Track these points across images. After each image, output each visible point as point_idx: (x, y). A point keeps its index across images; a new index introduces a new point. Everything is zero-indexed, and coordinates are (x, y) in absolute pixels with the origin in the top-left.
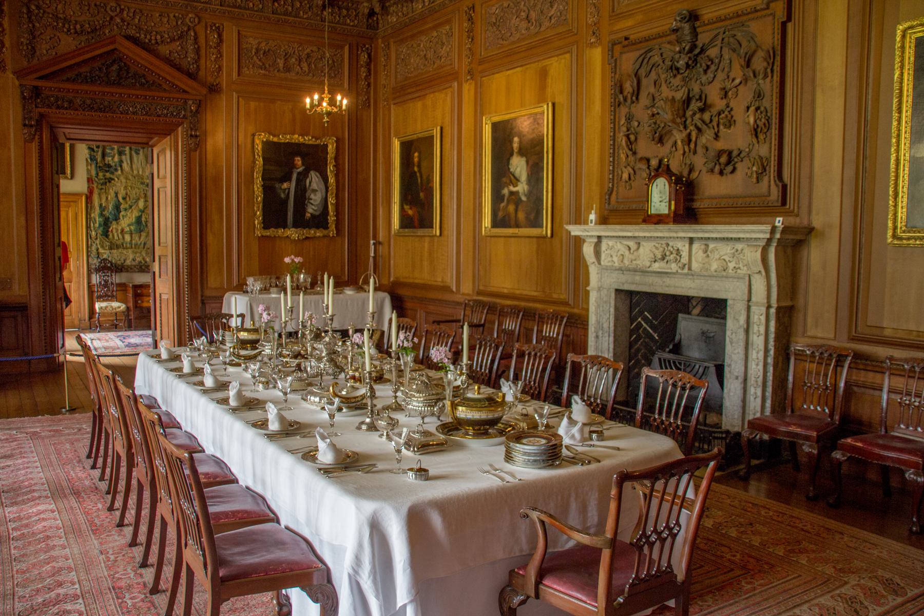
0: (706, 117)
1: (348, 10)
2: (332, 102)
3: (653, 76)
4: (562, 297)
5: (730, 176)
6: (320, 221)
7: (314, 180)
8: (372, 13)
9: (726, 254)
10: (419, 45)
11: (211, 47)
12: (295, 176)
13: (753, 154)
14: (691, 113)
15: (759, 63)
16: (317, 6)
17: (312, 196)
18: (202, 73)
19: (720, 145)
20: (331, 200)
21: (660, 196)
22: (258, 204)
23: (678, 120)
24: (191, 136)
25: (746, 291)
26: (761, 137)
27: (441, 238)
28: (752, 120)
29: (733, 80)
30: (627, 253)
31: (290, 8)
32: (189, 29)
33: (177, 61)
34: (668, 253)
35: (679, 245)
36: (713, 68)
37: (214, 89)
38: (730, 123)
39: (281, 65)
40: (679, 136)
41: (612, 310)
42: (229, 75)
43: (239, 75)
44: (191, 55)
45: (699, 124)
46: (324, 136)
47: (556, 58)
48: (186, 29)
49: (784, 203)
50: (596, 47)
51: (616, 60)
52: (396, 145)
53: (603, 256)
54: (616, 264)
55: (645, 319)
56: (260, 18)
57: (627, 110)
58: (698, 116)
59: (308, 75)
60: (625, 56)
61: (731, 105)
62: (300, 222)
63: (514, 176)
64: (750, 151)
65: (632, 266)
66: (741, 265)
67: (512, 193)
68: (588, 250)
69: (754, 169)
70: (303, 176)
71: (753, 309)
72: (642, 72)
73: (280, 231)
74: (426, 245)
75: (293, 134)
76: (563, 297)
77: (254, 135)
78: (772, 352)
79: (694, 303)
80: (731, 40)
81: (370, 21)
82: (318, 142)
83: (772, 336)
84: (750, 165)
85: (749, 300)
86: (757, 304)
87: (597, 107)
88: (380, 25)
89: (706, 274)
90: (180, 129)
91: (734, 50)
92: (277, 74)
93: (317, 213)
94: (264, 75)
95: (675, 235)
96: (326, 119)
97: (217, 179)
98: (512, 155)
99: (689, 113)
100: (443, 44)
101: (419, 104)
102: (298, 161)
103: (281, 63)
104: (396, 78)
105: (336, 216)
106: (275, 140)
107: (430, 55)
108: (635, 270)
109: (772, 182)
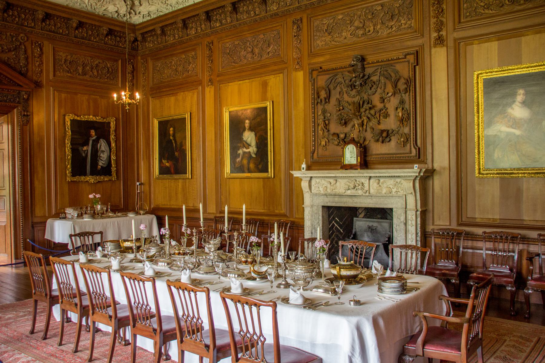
0: (372, 112)
1: (120, 38)
2: (132, 97)
3: (338, 89)
4: (281, 212)
5: (387, 144)
6: (106, 171)
7: (103, 145)
8: (136, 40)
9: (391, 184)
10: (171, 62)
11: (35, 57)
12: (91, 142)
13: (401, 132)
14: (364, 110)
15: (401, 86)
16: (102, 34)
17: (102, 155)
18: (30, 74)
19: (382, 127)
20: (113, 157)
21: (350, 154)
22: (68, 160)
23: (357, 114)
24: (24, 115)
25: (404, 204)
26: (405, 123)
27: (192, 180)
28: (400, 114)
29: (388, 93)
30: (329, 186)
31: (85, 35)
32: (20, 44)
33: (13, 65)
34: (357, 185)
35: (363, 180)
36: (375, 86)
37: (38, 85)
38: (387, 116)
39: (80, 71)
40: (356, 122)
41: (321, 218)
42: (48, 76)
43: (54, 76)
44: (22, 62)
45: (369, 116)
46: (107, 117)
47: (273, 76)
48: (19, 44)
49: (419, 158)
50: (299, 71)
51: (314, 79)
52: (156, 123)
53: (313, 188)
54: (322, 192)
55: (336, 222)
56: (67, 40)
57: (322, 107)
58: (367, 112)
59: (97, 77)
60: (319, 77)
61: (387, 106)
62: (95, 172)
63: (246, 142)
64: (399, 130)
65: (333, 193)
66: (399, 190)
67: (244, 153)
68: (304, 185)
69: (402, 140)
70: (96, 142)
71: (408, 212)
72: (331, 87)
73: (83, 178)
74: (180, 184)
75: (89, 115)
76: (283, 211)
77: (65, 116)
78: (419, 234)
79: (360, 212)
80: (385, 73)
81: (133, 45)
82: (105, 120)
83: (419, 226)
84: (400, 138)
85: (406, 208)
86: (410, 210)
87: (301, 104)
88: (140, 48)
89: (379, 195)
90: (15, 110)
91: (387, 78)
92: (78, 77)
93: (105, 166)
94: (70, 77)
95: (362, 175)
96: (127, 108)
97: (40, 144)
98: (244, 130)
99: (362, 110)
100: (190, 63)
101: (172, 99)
102: (93, 132)
103: (80, 69)
104: (153, 81)
105: (116, 167)
106: (79, 119)
107: (180, 69)
108: (335, 195)
109: (412, 146)
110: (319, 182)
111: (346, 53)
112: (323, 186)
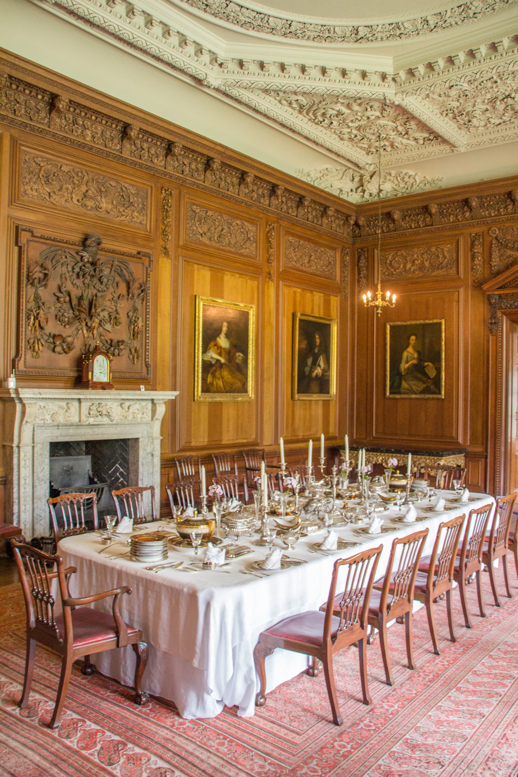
80: (118, 268)
110: (44, 407)
111: (68, 223)
112: (51, 414)
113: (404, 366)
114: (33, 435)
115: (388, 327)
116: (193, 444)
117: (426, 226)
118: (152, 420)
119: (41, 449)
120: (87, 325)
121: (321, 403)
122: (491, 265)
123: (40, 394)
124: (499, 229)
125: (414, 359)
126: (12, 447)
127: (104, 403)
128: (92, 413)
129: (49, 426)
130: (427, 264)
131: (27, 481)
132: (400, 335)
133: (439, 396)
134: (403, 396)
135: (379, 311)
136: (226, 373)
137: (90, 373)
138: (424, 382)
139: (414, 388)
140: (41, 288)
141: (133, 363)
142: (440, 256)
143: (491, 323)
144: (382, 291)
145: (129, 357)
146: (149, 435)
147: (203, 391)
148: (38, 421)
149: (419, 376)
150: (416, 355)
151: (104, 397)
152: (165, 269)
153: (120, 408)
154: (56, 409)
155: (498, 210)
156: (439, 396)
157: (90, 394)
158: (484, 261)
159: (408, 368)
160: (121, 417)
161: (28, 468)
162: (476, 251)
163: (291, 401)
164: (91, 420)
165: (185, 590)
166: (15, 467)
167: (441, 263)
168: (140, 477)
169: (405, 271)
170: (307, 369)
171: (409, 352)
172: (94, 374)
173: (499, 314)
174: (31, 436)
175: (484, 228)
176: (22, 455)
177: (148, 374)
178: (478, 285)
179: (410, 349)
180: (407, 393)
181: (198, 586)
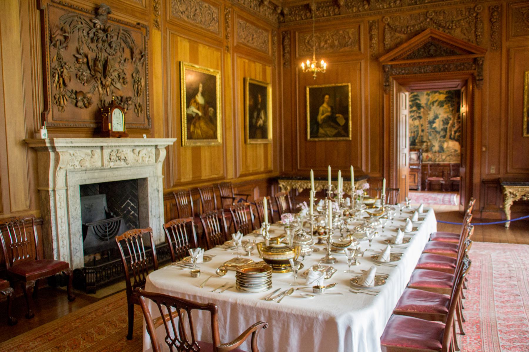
65: (94, 167)
112: (79, 160)
113: (320, 117)
114: (66, 179)
115: (308, 89)
116: (182, 180)
117: (335, 15)
118: (156, 162)
119: (73, 191)
120: (102, 83)
121: (262, 146)
122: (384, 44)
123: (72, 143)
124: (390, 18)
125: (328, 112)
126: (48, 191)
127: (121, 149)
128: (112, 158)
129: (78, 171)
130: (336, 43)
131: (63, 220)
132: (317, 96)
133: (347, 138)
134: (320, 139)
135: (315, 75)
136: (202, 124)
137: (110, 124)
138: (336, 129)
139: (329, 133)
140: (62, 50)
141: (138, 116)
142: (347, 37)
143: (385, 86)
144: (317, 59)
145: (135, 111)
146: (155, 175)
147: (188, 138)
148: (69, 167)
149: (332, 124)
150: (329, 109)
151: (122, 144)
152: (157, 38)
153: (132, 153)
154: (83, 156)
155: (389, 4)
156: (347, 138)
157: (111, 142)
158: (379, 40)
159: (324, 119)
160: (134, 161)
161: (63, 209)
162: (373, 33)
163: (244, 145)
164: (112, 165)
165: (320, 317)
166: (52, 208)
167: (347, 42)
168: (150, 209)
169: (320, 48)
170: (254, 121)
171: (324, 107)
172: (113, 125)
173: (391, 79)
174: (64, 180)
175: (379, 17)
176: (57, 197)
177: (149, 125)
178: (375, 58)
179: (325, 105)
180: (323, 137)
181: (334, 312)
